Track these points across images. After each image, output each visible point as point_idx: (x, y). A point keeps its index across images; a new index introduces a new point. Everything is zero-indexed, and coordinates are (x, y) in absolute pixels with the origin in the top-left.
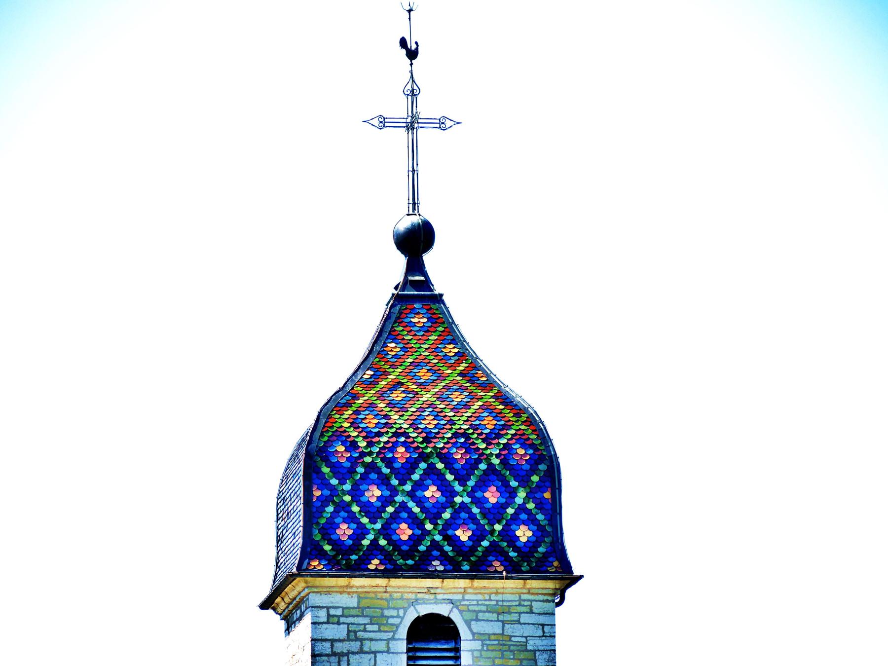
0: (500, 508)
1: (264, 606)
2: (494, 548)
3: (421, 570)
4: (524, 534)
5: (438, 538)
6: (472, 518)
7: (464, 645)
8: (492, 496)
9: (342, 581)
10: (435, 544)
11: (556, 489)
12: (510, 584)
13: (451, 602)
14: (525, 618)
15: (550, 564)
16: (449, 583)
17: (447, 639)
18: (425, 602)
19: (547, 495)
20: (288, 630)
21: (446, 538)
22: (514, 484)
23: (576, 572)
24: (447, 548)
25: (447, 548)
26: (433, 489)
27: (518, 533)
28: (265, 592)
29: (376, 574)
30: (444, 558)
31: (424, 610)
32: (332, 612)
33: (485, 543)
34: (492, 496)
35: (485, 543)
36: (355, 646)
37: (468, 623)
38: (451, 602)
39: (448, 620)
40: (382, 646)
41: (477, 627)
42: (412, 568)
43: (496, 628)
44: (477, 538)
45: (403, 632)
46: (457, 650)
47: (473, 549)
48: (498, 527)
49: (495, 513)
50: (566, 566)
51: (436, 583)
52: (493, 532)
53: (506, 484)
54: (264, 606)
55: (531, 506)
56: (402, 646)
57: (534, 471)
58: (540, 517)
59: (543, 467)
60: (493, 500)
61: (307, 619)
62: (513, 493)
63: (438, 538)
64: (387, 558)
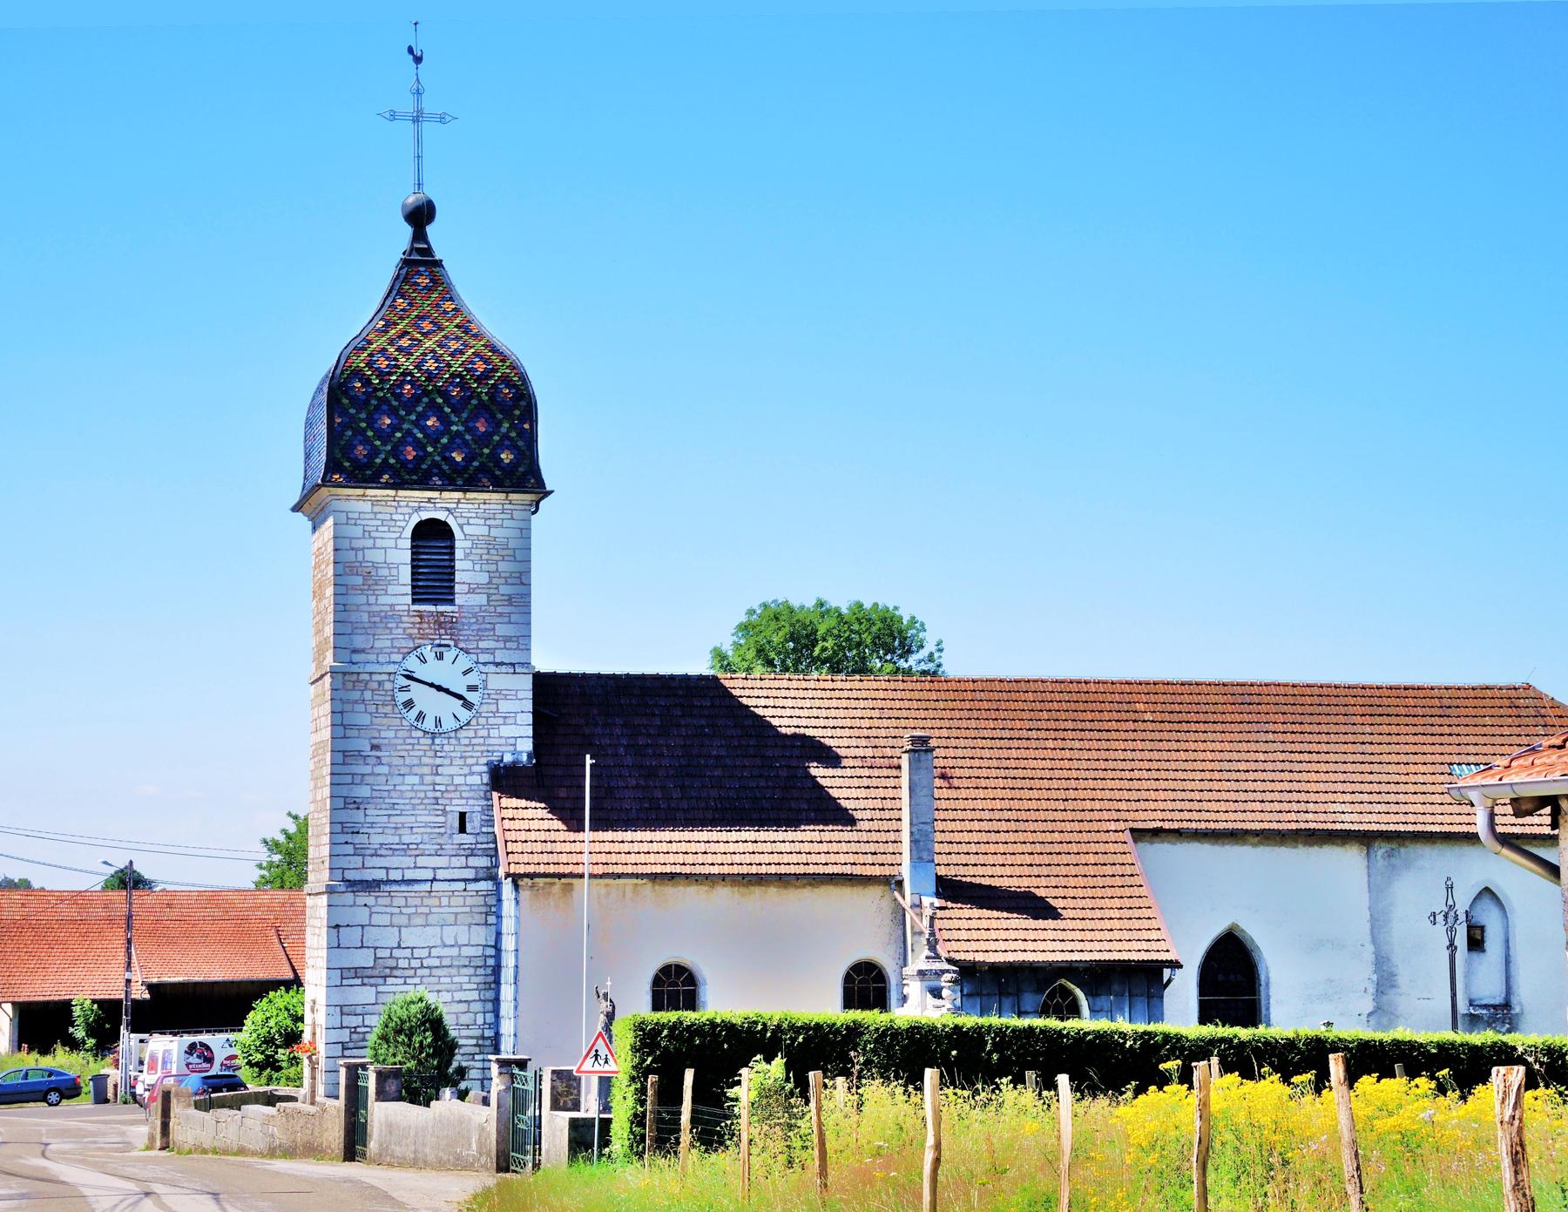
0: (488, 436)
1: (297, 508)
2: (482, 469)
3: (423, 483)
4: (506, 457)
5: (437, 458)
6: (466, 444)
7: (457, 544)
8: (482, 427)
9: (360, 491)
10: (435, 464)
11: (533, 421)
12: (495, 496)
13: (448, 509)
14: (506, 523)
15: (523, 478)
16: (446, 495)
17: (444, 539)
18: (426, 509)
19: (526, 426)
20: (314, 529)
21: (444, 458)
22: (500, 416)
23: (548, 488)
24: (445, 467)
25: (445, 467)
26: (459, 459)
27: (503, 456)
28: (296, 499)
29: (387, 486)
30: (442, 475)
31: (425, 516)
32: (380, 953)
33: (476, 464)
34: (482, 427)
35: (476, 464)
36: (369, 543)
37: (461, 526)
38: (448, 509)
39: (445, 524)
40: (391, 543)
41: (467, 529)
42: (415, 482)
43: (485, 530)
44: (468, 460)
45: (408, 533)
46: (452, 547)
47: (465, 468)
48: (486, 451)
49: (484, 439)
50: (540, 483)
51: (435, 494)
52: (482, 454)
53: (493, 416)
54: (297, 508)
55: (513, 434)
56: (408, 544)
57: (516, 406)
58: (520, 443)
59: (523, 403)
60: (483, 429)
61: (330, 521)
62: (499, 424)
63: (437, 458)
64: (395, 474)
